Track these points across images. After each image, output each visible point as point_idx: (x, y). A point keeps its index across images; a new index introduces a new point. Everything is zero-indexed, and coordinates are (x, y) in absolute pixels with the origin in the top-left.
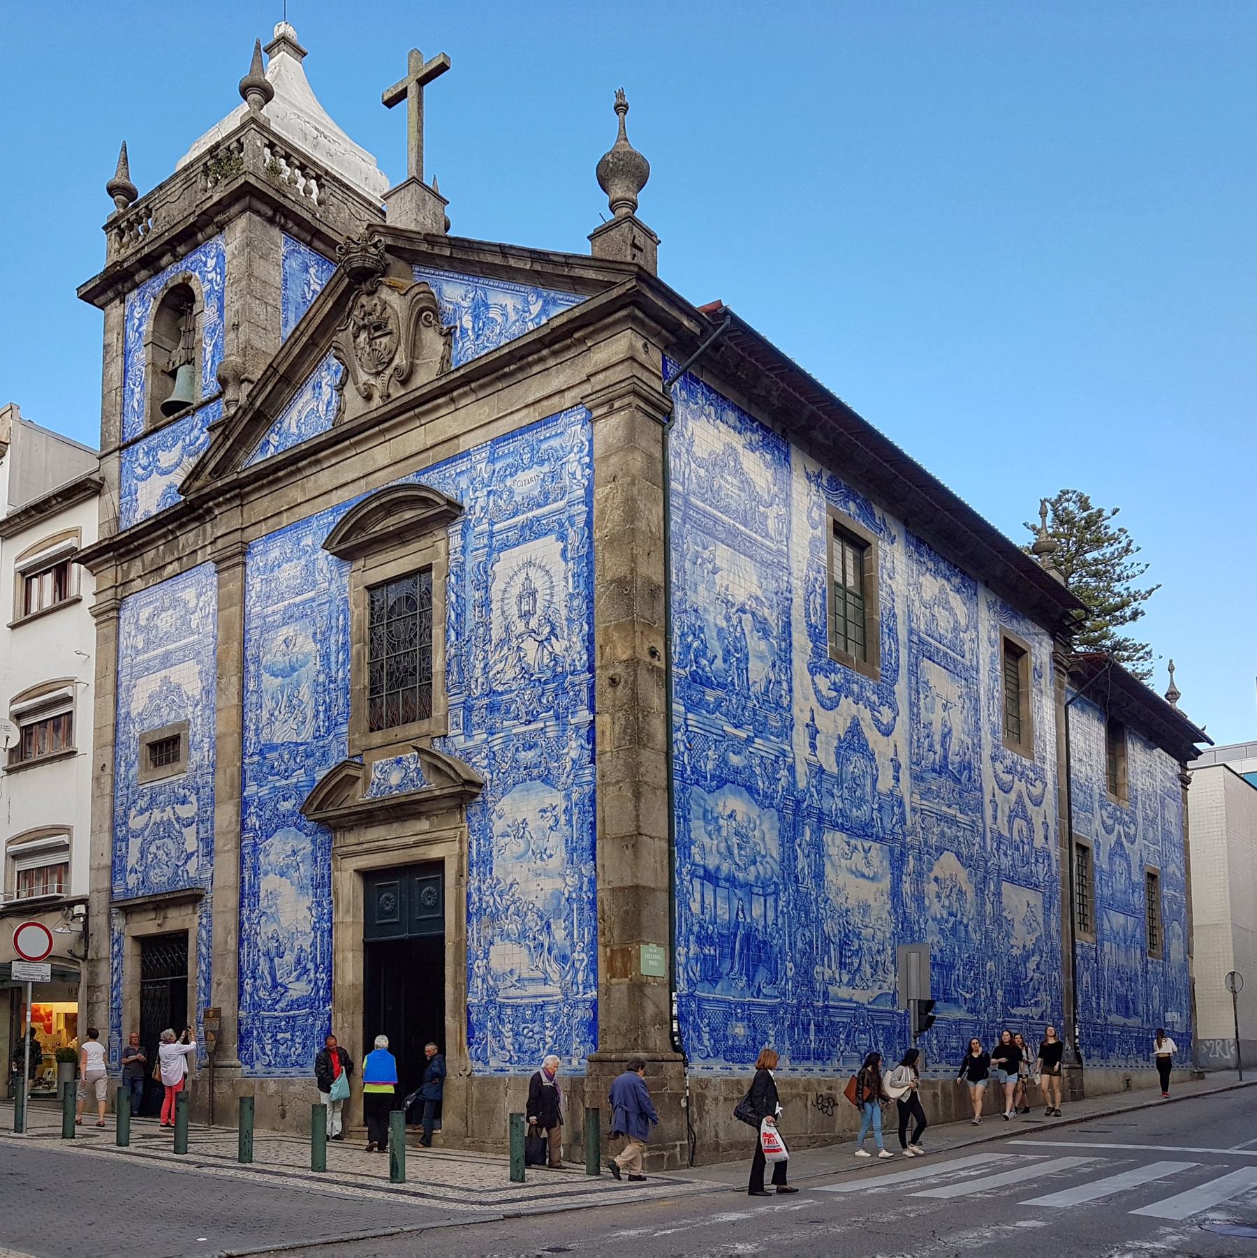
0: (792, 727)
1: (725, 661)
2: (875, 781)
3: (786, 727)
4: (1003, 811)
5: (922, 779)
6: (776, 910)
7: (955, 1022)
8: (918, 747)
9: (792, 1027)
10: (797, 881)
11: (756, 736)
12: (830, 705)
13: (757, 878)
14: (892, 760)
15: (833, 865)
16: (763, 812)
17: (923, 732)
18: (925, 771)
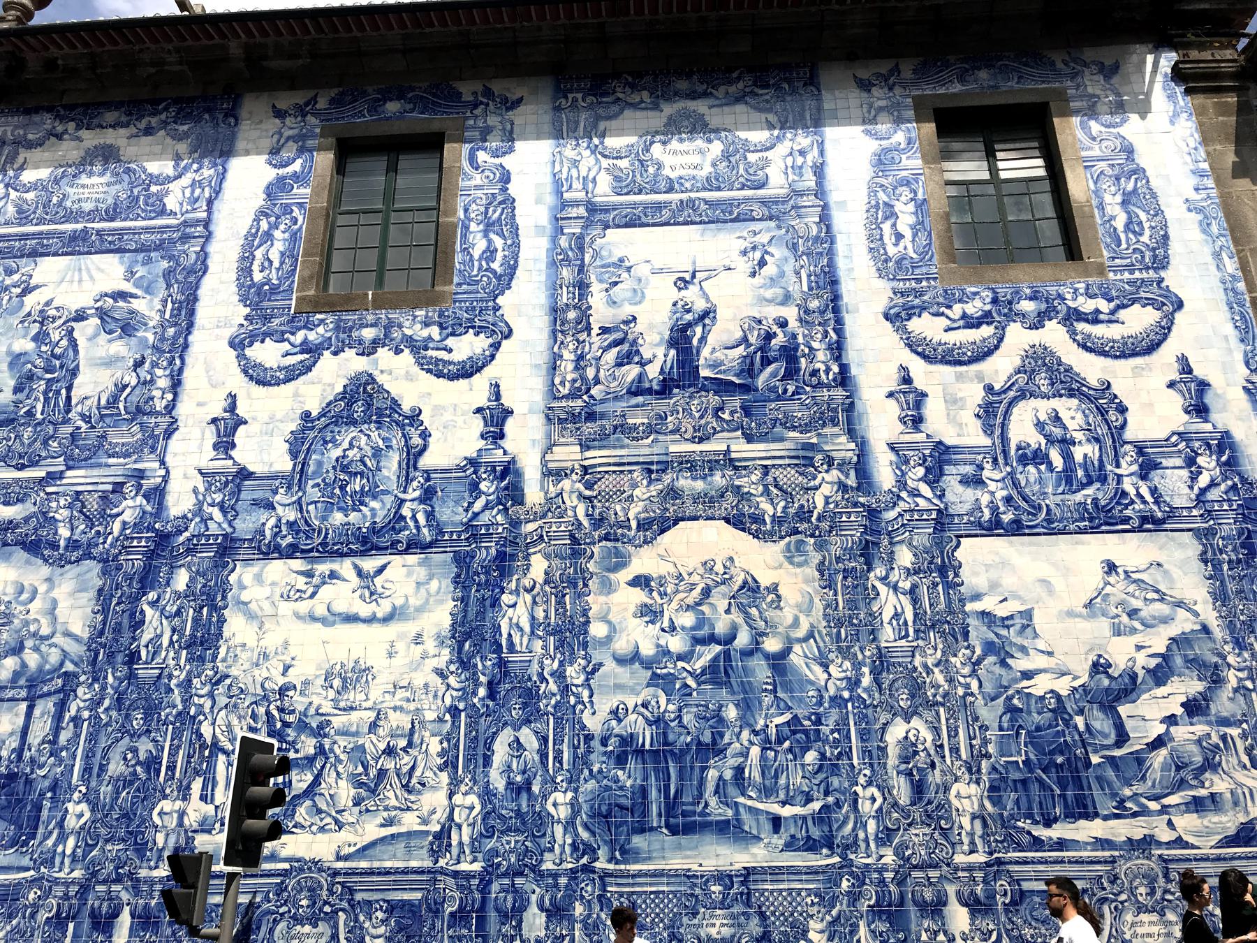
0: (168, 434)
1: (17, 390)
2: (413, 456)
3: (158, 436)
4: (953, 401)
5: (591, 417)
6: (59, 717)
7: (724, 878)
8: (577, 368)
9: (59, 922)
10: (133, 657)
11: (69, 468)
12: (291, 374)
13: (16, 675)
14: (479, 410)
15: (251, 616)
16: (59, 570)
17: (596, 341)
18: (602, 401)
